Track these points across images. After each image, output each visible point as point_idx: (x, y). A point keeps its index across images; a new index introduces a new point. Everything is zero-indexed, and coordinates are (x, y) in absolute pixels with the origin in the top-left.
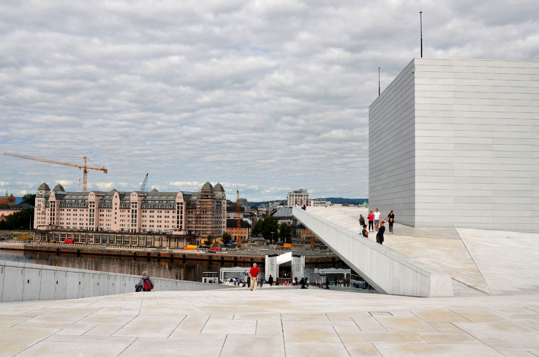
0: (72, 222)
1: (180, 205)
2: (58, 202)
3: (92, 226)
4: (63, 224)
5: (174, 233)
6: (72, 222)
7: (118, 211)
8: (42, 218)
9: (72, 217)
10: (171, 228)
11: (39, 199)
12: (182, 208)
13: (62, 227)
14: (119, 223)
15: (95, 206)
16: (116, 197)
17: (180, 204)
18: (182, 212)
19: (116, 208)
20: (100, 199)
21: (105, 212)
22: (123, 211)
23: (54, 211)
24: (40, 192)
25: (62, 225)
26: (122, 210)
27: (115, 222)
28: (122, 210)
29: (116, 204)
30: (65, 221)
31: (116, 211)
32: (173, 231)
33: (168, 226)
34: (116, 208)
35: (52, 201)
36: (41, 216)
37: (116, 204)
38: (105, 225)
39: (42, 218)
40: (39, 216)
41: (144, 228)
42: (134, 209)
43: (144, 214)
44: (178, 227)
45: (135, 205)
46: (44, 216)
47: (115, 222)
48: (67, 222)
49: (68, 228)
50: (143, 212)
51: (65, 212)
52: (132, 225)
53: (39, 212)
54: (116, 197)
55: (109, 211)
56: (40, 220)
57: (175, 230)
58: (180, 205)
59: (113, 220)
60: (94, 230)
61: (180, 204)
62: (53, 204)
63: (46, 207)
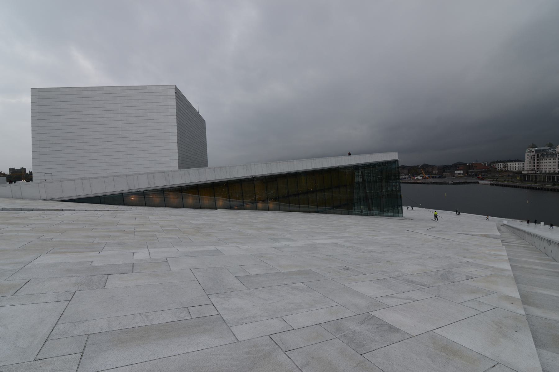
2: (538, 155)
4: (542, 169)
6: (548, 167)
8: (529, 166)
9: (548, 164)
11: (528, 154)
13: (542, 171)
23: (535, 161)
24: (529, 150)
25: (542, 170)
30: (543, 167)
35: (533, 154)
36: (529, 165)
39: (529, 166)
40: (527, 165)
46: (530, 165)
49: (554, 171)
51: (544, 161)
53: (528, 162)
56: (529, 167)
62: (534, 156)
63: (531, 158)
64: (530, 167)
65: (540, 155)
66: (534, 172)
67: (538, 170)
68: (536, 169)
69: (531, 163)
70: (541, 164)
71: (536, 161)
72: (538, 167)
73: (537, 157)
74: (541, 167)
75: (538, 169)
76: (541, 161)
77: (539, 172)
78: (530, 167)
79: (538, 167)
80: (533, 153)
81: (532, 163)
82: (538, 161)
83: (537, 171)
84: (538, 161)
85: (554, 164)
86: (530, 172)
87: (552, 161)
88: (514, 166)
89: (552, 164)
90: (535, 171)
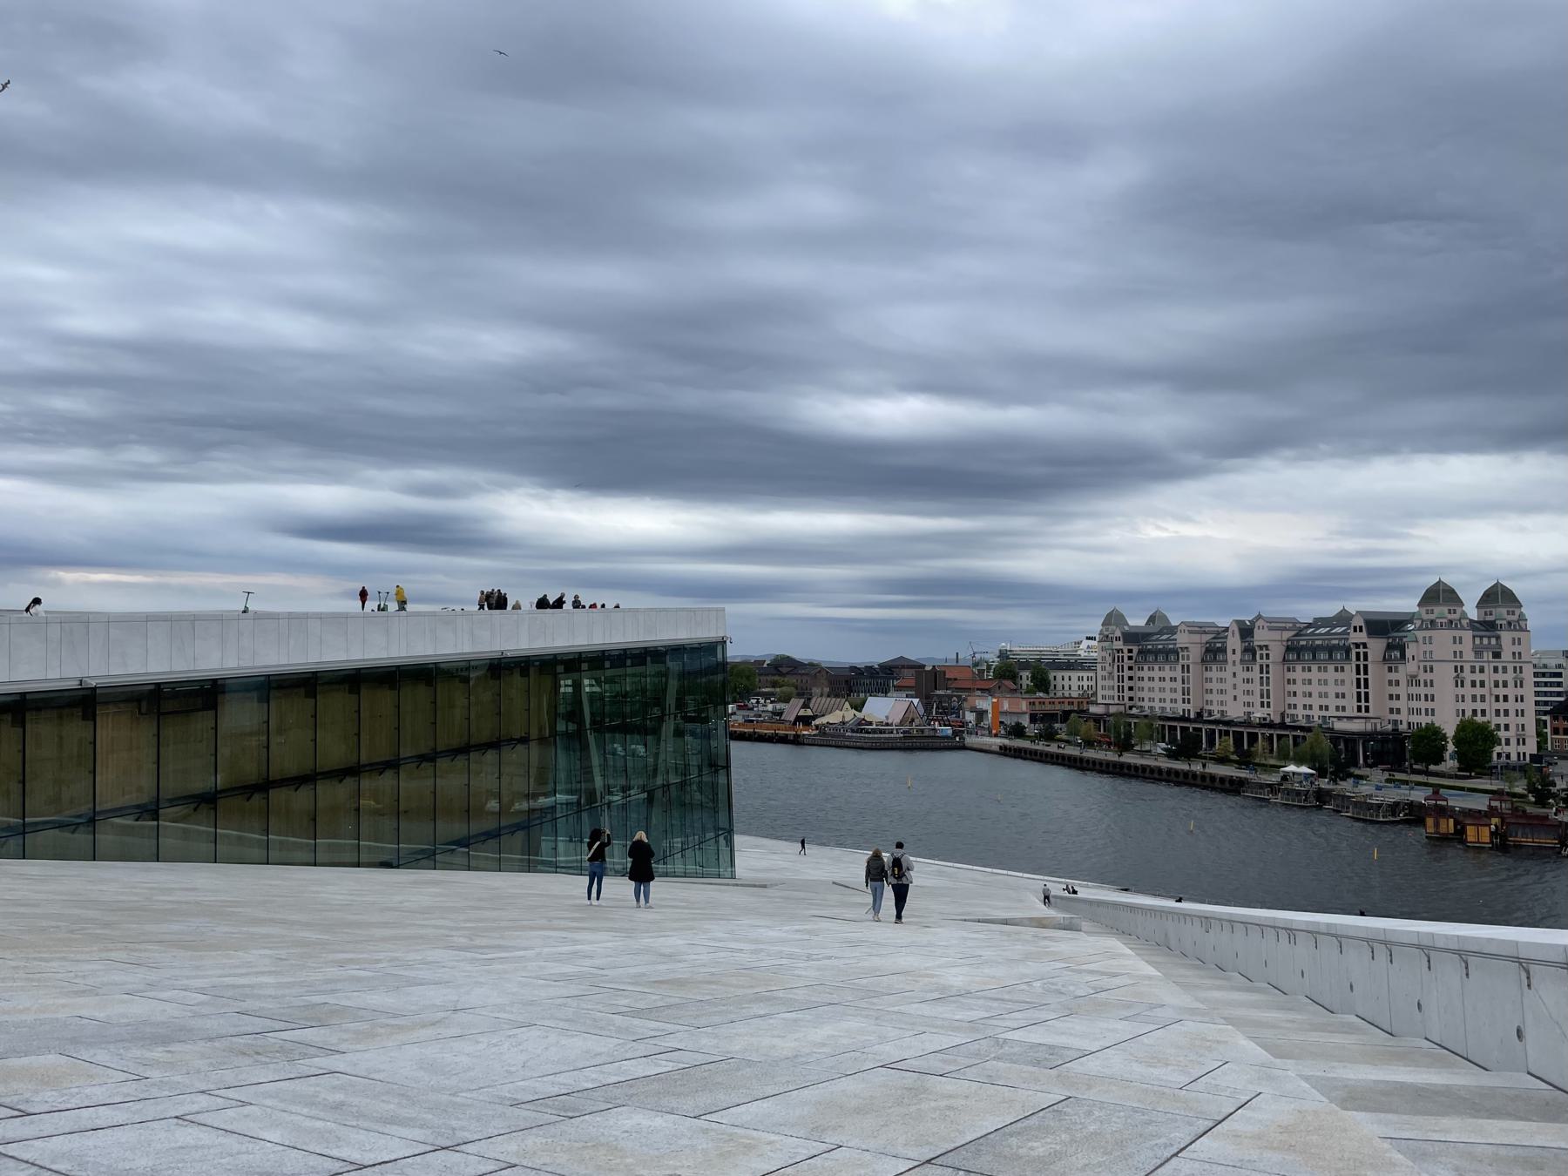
0: (1157, 695)
1: (1361, 650)
2: (1130, 651)
3: (1186, 706)
5: (1339, 726)
6: (1157, 695)
7: (1239, 668)
10: (1332, 712)
12: (1366, 658)
14: (1243, 698)
15: (1191, 657)
16: (1233, 634)
17: (1361, 647)
18: (1366, 667)
19: (1234, 662)
20: (1285, 638)
21: (1214, 673)
22: (1248, 670)
26: (1245, 666)
27: (1235, 698)
28: (1245, 666)
29: (1234, 652)
31: (1234, 669)
32: (1335, 720)
33: (1344, 708)
34: (1234, 662)
35: (1118, 648)
37: (1234, 652)
38: (1215, 703)
40: (1104, 683)
41: (1292, 711)
42: (1265, 661)
43: (1291, 675)
44: (1359, 709)
45: (1264, 652)
46: (1111, 683)
47: (1235, 698)
48: (1338, 704)
50: (1289, 670)
51: (1146, 674)
52: (1262, 704)
53: (1104, 673)
54: (1233, 634)
55: (1221, 670)
57: (1339, 718)
58: (1361, 650)
59: (1231, 693)
60: (1192, 716)
61: (1361, 647)
62: (1121, 655)
64: (1111, 693)
65: (1135, 649)
66: (1122, 709)
67: (1131, 703)
68: (1126, 699)
69: (1113, 679)
70: (1140, 684)
71: (1127, 673)
72: (1131, 694)
73: (1130, 658)
74: (1140, 694)
75: (1131, 699)
76: (1141, 674)
77: (1134, 711)
78: (1111, 693)
79: (1131, 694)
80: (1118, 643)
81: (1116, 678)
82: (1131, 673)
83: (1131, 708)
84: (1131, 673)
85: (1173, 685)
86: (1112, 710)
87: (1167, 673)
88: (1066, 683)
89: (1168, 685)
90: (1124, 704)
